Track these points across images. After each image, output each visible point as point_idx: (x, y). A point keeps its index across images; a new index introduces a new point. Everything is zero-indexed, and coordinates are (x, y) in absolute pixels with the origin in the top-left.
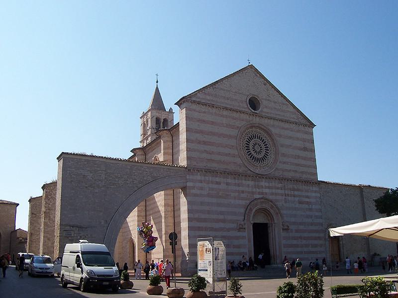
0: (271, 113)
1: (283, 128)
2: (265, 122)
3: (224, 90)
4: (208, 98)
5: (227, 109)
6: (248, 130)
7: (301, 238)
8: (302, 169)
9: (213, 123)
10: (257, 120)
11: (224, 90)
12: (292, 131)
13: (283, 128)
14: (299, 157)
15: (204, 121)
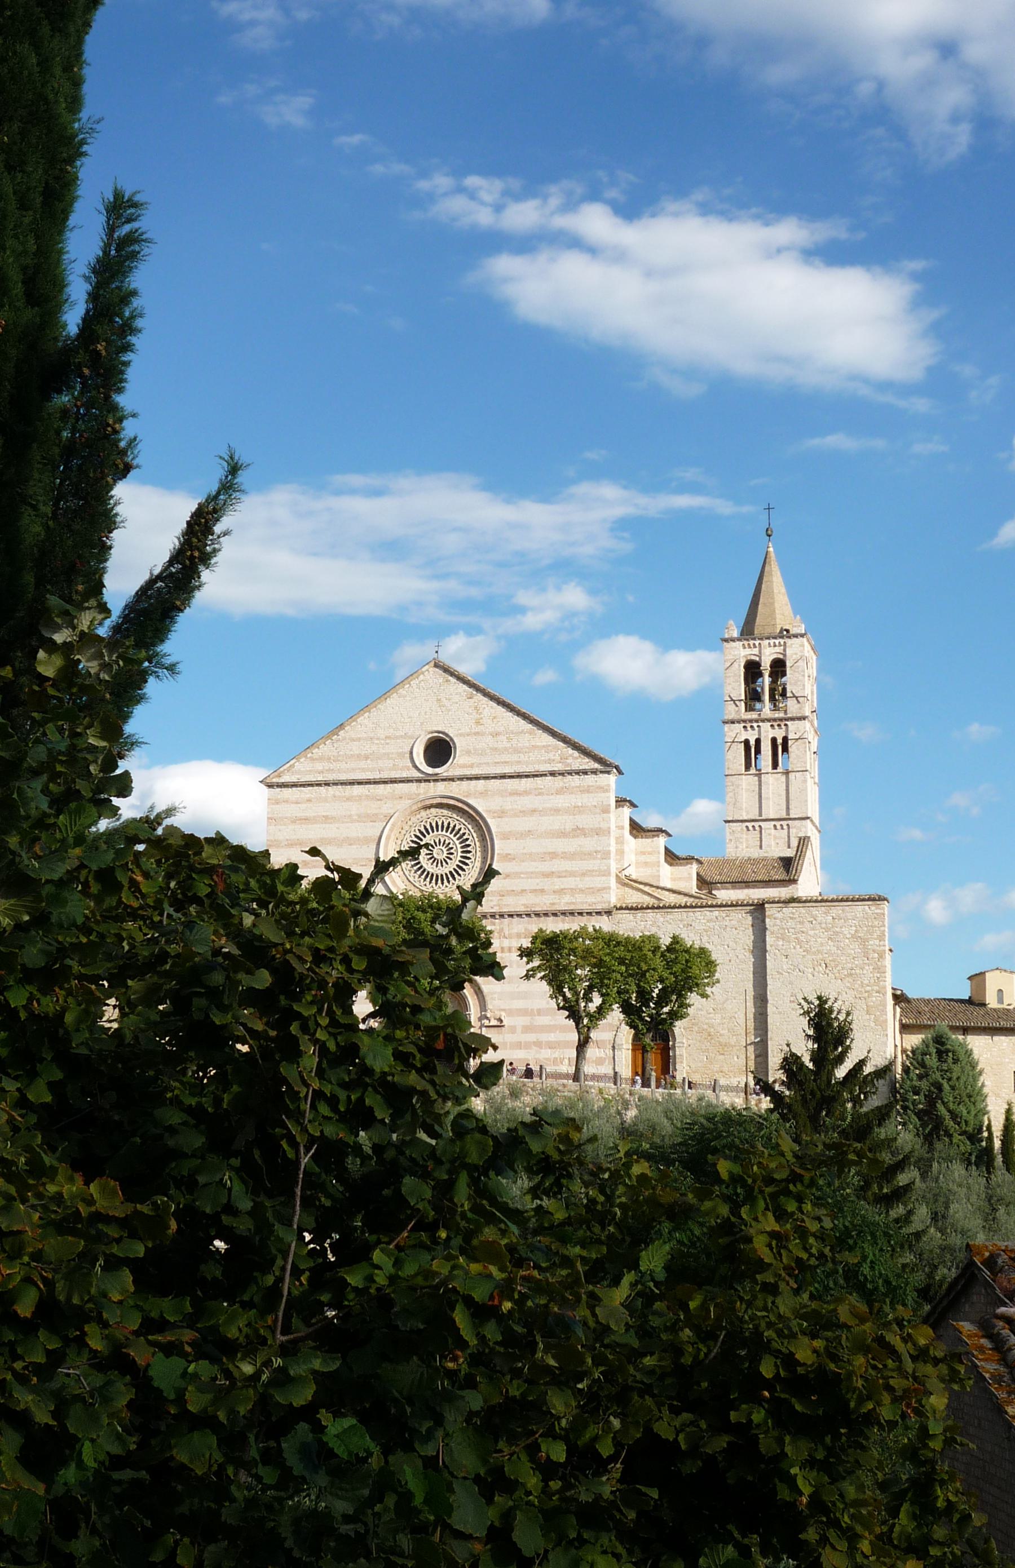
0: (479, 765)
1: (517, 793)
2: (456, 790)
3: (359, 739)
4: (319, 766)
5: (360, 783)
6: (418, 816)
7: (539, 1044)
8: (558, 884)
9: (327, 819)
10: (441, 789)
11: (359, 739)
12: (540, 794)
13: (517, 793)
14: (554, 855)
15: (306, 820)
